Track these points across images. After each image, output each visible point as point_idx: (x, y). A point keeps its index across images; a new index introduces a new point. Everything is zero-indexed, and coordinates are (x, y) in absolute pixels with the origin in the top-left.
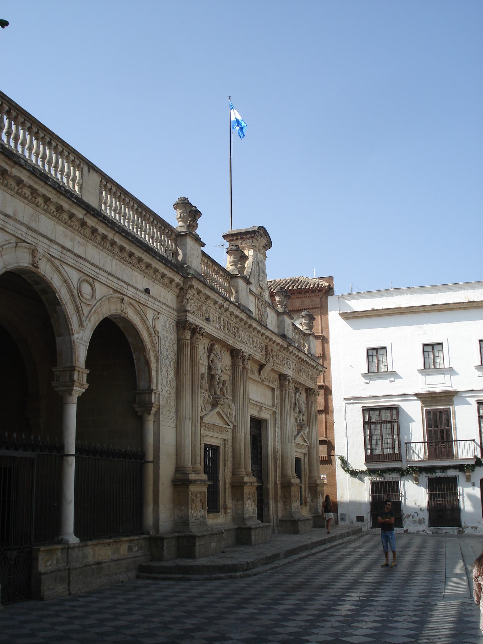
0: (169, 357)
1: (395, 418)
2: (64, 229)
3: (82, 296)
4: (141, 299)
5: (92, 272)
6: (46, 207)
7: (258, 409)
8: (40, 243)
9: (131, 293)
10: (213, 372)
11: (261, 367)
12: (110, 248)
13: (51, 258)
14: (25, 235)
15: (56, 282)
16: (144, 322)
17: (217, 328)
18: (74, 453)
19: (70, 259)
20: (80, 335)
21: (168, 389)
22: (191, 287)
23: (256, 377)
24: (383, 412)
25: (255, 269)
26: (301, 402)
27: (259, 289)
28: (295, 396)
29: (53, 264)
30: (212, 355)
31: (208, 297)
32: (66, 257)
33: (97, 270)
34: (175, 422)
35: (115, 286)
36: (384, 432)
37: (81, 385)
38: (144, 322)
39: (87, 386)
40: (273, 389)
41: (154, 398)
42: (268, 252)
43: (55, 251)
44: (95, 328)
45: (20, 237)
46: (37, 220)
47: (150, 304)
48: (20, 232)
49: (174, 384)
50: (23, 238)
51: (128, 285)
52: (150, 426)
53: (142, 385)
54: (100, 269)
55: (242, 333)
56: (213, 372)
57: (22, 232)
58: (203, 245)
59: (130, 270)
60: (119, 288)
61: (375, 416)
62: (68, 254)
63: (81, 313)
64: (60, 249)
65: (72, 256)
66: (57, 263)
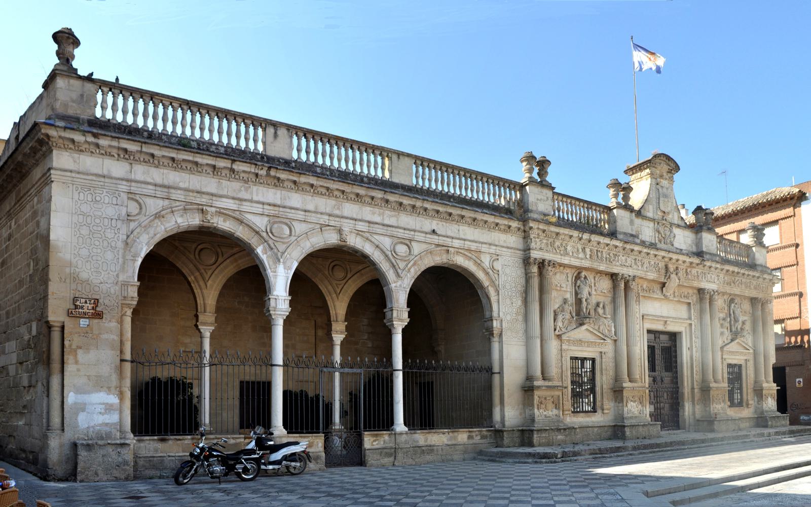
0: (514, 289)
2: (372, 209)
3: (397, 254)
4: (471, 247)
5: (407, 235)
6: (345, 197)
7: (662, 323)
8: (345, 224)
9: (457, 244)
10: (579, 296)
11: (663, 285)
12: (424, 213)
13: (359, 233)
14: (328, 221)
15: (368, 249)
16: (479, 265)
17: (582, 259)
18: (401, 368)
19: (379, 229)
21: (514, 315)
22: (531, 228)
23: (659, 295)
25: (653, 195)
26: (736, 312)
27: (660, 213)
28: (730, 307)
29: (362, 236)
30: (579, 282)
31: (557, 234)
32: (374, 229)
33: (412, 233)
34: (525, 340)
35: (436, 242)
38: (479, 265)
40: (689, 304)
41: (495, 324)
42: (676, 176)
43: (362, 226)
44: (416, 277)
45: (324, 223)
46: (341, 207)
47: (483, 250)
48: (322, 220)
49: (523, 311)
50: (327, 224)
53: (487, 314)
54: (415, 231)
55: (623, 258)
57: (324, 219)
58: (554, 188)
59: (456, 226)
60: (441, 242)
62: (376, 226)
63: (397, 267)
64: (367, 224)
65: (381, 227)
66: (367, 235)
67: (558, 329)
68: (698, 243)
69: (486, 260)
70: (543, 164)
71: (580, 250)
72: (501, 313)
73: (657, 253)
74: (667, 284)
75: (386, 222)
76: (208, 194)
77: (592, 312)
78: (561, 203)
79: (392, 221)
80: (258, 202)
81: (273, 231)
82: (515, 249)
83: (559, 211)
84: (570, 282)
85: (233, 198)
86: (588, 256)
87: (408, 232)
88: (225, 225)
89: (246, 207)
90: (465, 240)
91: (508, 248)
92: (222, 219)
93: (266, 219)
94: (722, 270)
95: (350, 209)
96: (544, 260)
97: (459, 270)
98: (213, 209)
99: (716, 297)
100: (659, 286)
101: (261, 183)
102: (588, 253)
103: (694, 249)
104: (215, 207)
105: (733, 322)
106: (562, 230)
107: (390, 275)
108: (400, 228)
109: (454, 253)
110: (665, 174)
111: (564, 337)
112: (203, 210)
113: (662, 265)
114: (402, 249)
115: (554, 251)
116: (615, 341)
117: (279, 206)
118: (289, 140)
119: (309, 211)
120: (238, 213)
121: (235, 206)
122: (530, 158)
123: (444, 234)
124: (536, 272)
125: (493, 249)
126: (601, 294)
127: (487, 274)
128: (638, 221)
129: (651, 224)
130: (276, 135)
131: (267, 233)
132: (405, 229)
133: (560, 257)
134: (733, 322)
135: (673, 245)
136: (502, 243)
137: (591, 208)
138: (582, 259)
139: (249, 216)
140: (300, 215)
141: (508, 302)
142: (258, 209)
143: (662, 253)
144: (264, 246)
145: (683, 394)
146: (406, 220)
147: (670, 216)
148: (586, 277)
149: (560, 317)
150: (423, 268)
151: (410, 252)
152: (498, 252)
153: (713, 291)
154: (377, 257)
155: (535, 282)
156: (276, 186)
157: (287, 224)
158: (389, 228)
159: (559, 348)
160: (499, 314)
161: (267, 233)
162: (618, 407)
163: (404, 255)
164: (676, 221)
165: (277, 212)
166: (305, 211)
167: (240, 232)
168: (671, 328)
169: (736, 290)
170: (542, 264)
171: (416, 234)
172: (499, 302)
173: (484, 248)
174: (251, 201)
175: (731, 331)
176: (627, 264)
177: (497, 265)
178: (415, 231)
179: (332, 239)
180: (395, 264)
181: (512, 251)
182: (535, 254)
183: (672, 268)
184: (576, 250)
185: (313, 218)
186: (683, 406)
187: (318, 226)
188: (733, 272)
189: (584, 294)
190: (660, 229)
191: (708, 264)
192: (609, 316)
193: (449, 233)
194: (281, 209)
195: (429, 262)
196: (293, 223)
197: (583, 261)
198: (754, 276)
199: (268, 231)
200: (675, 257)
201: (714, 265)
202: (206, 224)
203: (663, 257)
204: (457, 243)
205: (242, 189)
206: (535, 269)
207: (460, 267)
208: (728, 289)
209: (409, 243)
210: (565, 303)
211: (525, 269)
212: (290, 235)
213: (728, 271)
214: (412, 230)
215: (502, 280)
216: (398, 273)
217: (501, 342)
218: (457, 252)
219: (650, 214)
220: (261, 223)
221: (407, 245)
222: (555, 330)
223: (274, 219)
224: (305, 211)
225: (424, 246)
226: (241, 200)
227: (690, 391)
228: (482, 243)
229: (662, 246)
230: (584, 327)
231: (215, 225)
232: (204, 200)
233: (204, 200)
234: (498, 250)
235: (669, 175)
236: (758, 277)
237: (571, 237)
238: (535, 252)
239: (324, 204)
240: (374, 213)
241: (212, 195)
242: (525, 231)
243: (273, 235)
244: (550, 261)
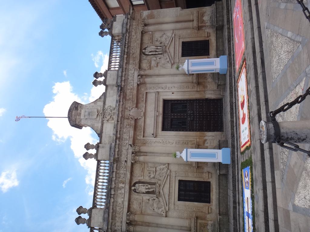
67: (162, 213)
70: (80, 210)
77: (153, 181)
84: (138, 197)
86: (123, 185)
96: (127, 223)
105: (157, 53)
115: (122, 212)
122: (79, 221)
126: (143, 172)
133: (124, 209)
147: (99, 108)
153: (138, 76)
164: (101, 104)
175: (161, 54)
184: (120, 195)
190: (106, 119)
219: (100, 125)
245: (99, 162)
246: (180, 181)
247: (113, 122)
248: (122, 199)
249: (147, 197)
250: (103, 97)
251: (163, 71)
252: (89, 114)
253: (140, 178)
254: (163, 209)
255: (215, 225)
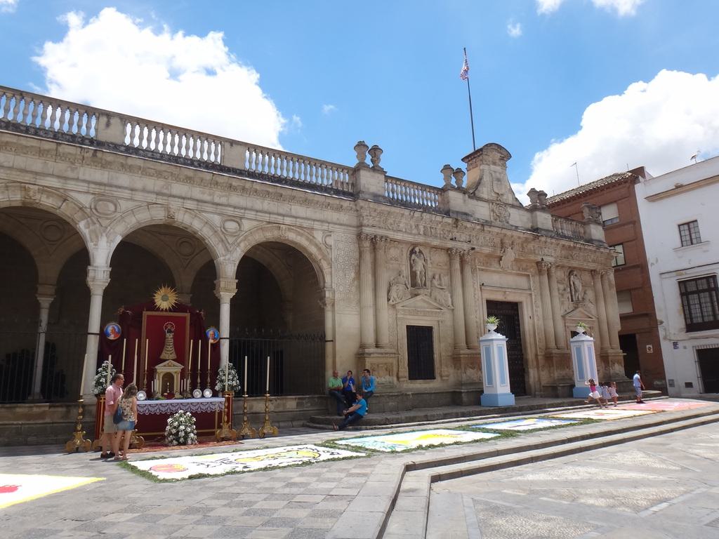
1: (713, 286)
10: (414, 269)
11: (500, 259)
16: (311, 240)
17: (415, 235)
19: (209, 208)
20: (227, 257)
22: (362, 207)
24: (699, 282)
27: (493, 194)
29: (190, 213)
30: (413, 256)
31: (389, 213)
33: (243, 211)
35: (267, 219)
36: (703, 300)
37: (227, 290)
39: (236, 291)
41: (328, 294)
42: (508, 163)
43: (190, 204)
51: (284, 216)
52: (329, 315)
54: (245, 209)
56: (414, 269)
57: (152, 198)
61: (692, 287)
64: (196, 203)
68: (534, 220)
69: (319, 236)
70: (375, 151)
71: (414, 227)
72: (333, 284)
73: (490, 229)
74: (503, 258)
75: (217, 200)
76: (32, 172)
77: (428, 283)
78: (395, 186)
79: (223, 200)
80: (84, 181)
81: (98, 208)
82: (347, 226)
83: (393, 193)
85: (58, 177)
86: (422, 232)
87: (238, 210)
88: (47, 202)
89: (71, 185)
90: (296, 218)
91: (341, 225)
92: (45, 196)
93: (91, 197)
94: (558, 244)
95: (179, 188)
97: (292, 245)
98: (37, 187)
99: (553, 270)
100: (497, 260)
101: (88, 165)
102: (422, 229)
103: (529, 225)
104: (38, 185)
105: (573, 293)
106: (393, 209)
107: (219, 250)
108: (230, 206)
109: (285, 230)
110: (497, 161)
111: (399, 307)
112: (25, 187)
113: (497, 240)
114: (231, 226)
116: (453, 310)
117: (105, 185)
118: (121, 127)
119: (136, 190)
120: (62, 191)
121: (59, 184)
122: (361, 145)
123: (276, 211)
124: (370, 245)
125: (325, 227)
127: (320, 249)
128: (474, 202)
129: (485, 205)
130: (108, 125)
131: (91, 209)
132: (235, 208)
133: (392, 233)
134: (573, 293)
135: (508, 222)
136: (335, 220)
137: (425, 190)
138: (415, 235)
139: (72, 194)
140: (126, 194)
141: (341, 274)
142: (83, 187)
143: (496, 230)
144: (88, 221)
145: (527, 361)
146: (236, 199)
147: (505, 197)
148: (420, 252)
149: (394, 288)
150: (254, 243)
151: (240, 228)
152: (331, 229)
154: (205, 232)
155: (368, 257)
156: (104, 168)
157: (112, 202)
158: (219, 207)
159: (395, 317)
160: (331, 285)
161: (91, 209)
162: (457, 373)
163: (234, 231)
164: (510, 201)
165: (102, 191)
166: (132, 190)
167: (65, 210)
168: (511, 298)
169: (575, 264)
170: (374, 240)
171: (247, 212)
172: (331, 274)
173: (317, 225)
174: (77, 179)
175: (572, 301)
176: (462, 240)
177: (330, 241)
178: (245, 209)
179: (159, 216)
180: (224, 239)
181: (345, 227)
182: (367, 230)
183: (507, 241)
185: (139, 196)
186: (528, 372)
187: (146, 204)
188: (570, 247)
189: (419, 268)
191: (543, 239)
192: (445, 287)
193: (281, 211)
194: (107, 188)
195: (260, 237)
196: (119, 201)
197: (416, 237)
198: (590, 250)
199: (92, 207)
200: (509, 233)
201: (549, 240)
202: (28, 200)
203: (498, 234)
204: (288, 220)
205: (69, 169)
206: (367, 244)
207: (293, 242)
208: (565, 262)
209: (239, 221)
210: (400, 275)
211: (359, 244)
212: (115, 211)
213: (563, 246)
214: (242, 209)
215: (334, 255)
216: (226, 247)
217: (333, 311)
218: (289, 229)
219: (485, 196)
220: (85, 200)
221: (237, 222)
222: (389, 300)
223: (100, 197)
224: (132, 190)
225: (255, 223)
226: (66, 178)
227: (533, 357)
228: (314, 220)
229: (498, 223)
230: (418, 298)
231: (37, 201)
232: (28, 178)
233: (26, 178)
234: (331, 227)
235: (502, 162)
236: (595, 252)
237: (403, 215)
238: (367, 229)
239: (152, 183)
240: (203, 193)
241: (36, 173)
242: (357, 211)
243: (97, 212)
244: (382, 237)
245: (442, 191)
246: (430, 329)
247: (492, 219)
248: (404, 230)
249: (406, 272)
250: (518, 205)
251: (557, 301)
252: (499, 180)
253: (428, 259)
254: (398, 300)
255: (392, 387)
